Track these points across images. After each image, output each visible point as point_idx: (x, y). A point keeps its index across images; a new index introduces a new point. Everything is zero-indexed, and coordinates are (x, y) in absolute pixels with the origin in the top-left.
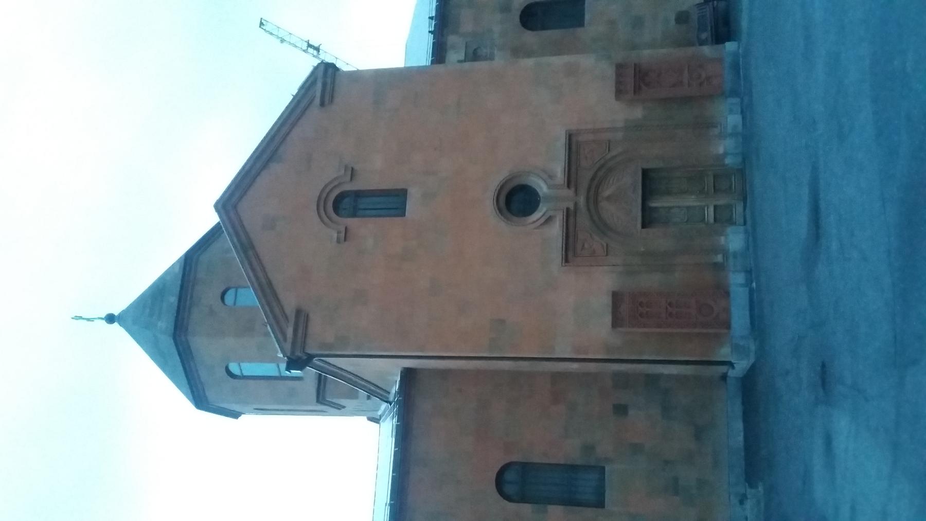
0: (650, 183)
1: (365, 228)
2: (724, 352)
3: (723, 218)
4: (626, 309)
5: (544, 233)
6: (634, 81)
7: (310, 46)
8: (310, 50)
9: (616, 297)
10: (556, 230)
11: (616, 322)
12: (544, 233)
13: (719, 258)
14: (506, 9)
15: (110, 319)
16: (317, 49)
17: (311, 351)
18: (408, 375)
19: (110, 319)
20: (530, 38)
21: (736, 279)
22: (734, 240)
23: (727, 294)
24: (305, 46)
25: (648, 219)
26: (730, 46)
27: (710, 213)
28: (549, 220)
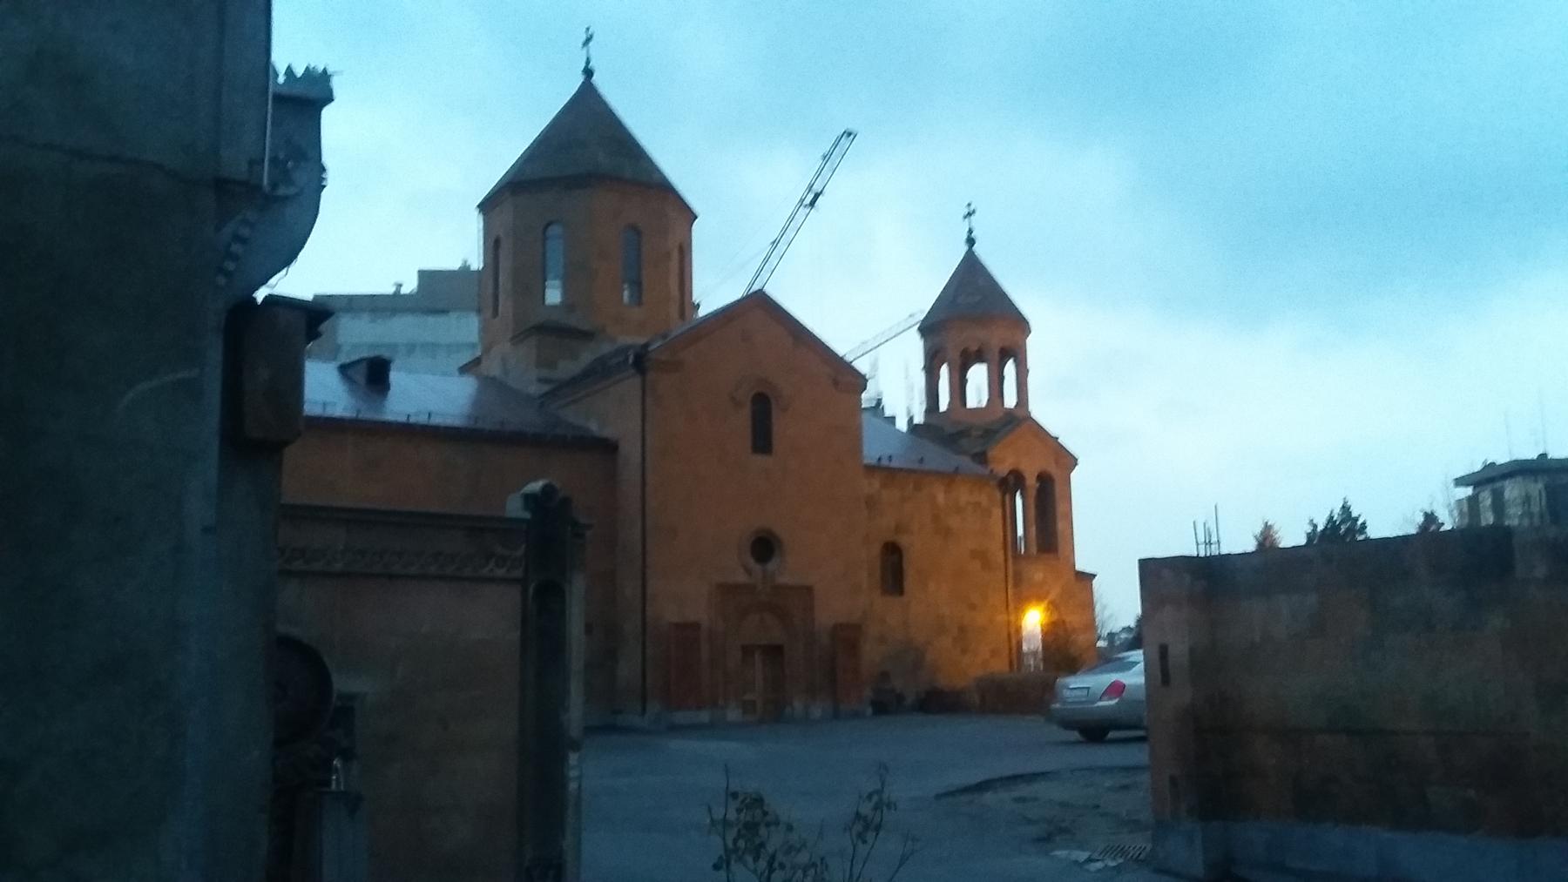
0: (774, 652)
1: (742, 420)
2: (654, 707)
3: (748, 707)
4: (687, 632)
5: (737, 569)
6: (848, 637)
7: (817, 196)
8: (811, 197)
9: (695, 626)
10: (742, 578)
11: (677, 625)
12: (737, 569)
13: (721, 702)
14: (899, 529)
15: (588, 73)
16: (812, 204)
17: (651, 376)
18: (609, 448)
19: (588, 73)
20: (876, 549)
21: (704, 716)
22: (733, 714)
23: (699, 708)
24: (817, 188)
25: (747, 651)
26: (869, 711)
27: (748, 697)
28: (748, 571)
